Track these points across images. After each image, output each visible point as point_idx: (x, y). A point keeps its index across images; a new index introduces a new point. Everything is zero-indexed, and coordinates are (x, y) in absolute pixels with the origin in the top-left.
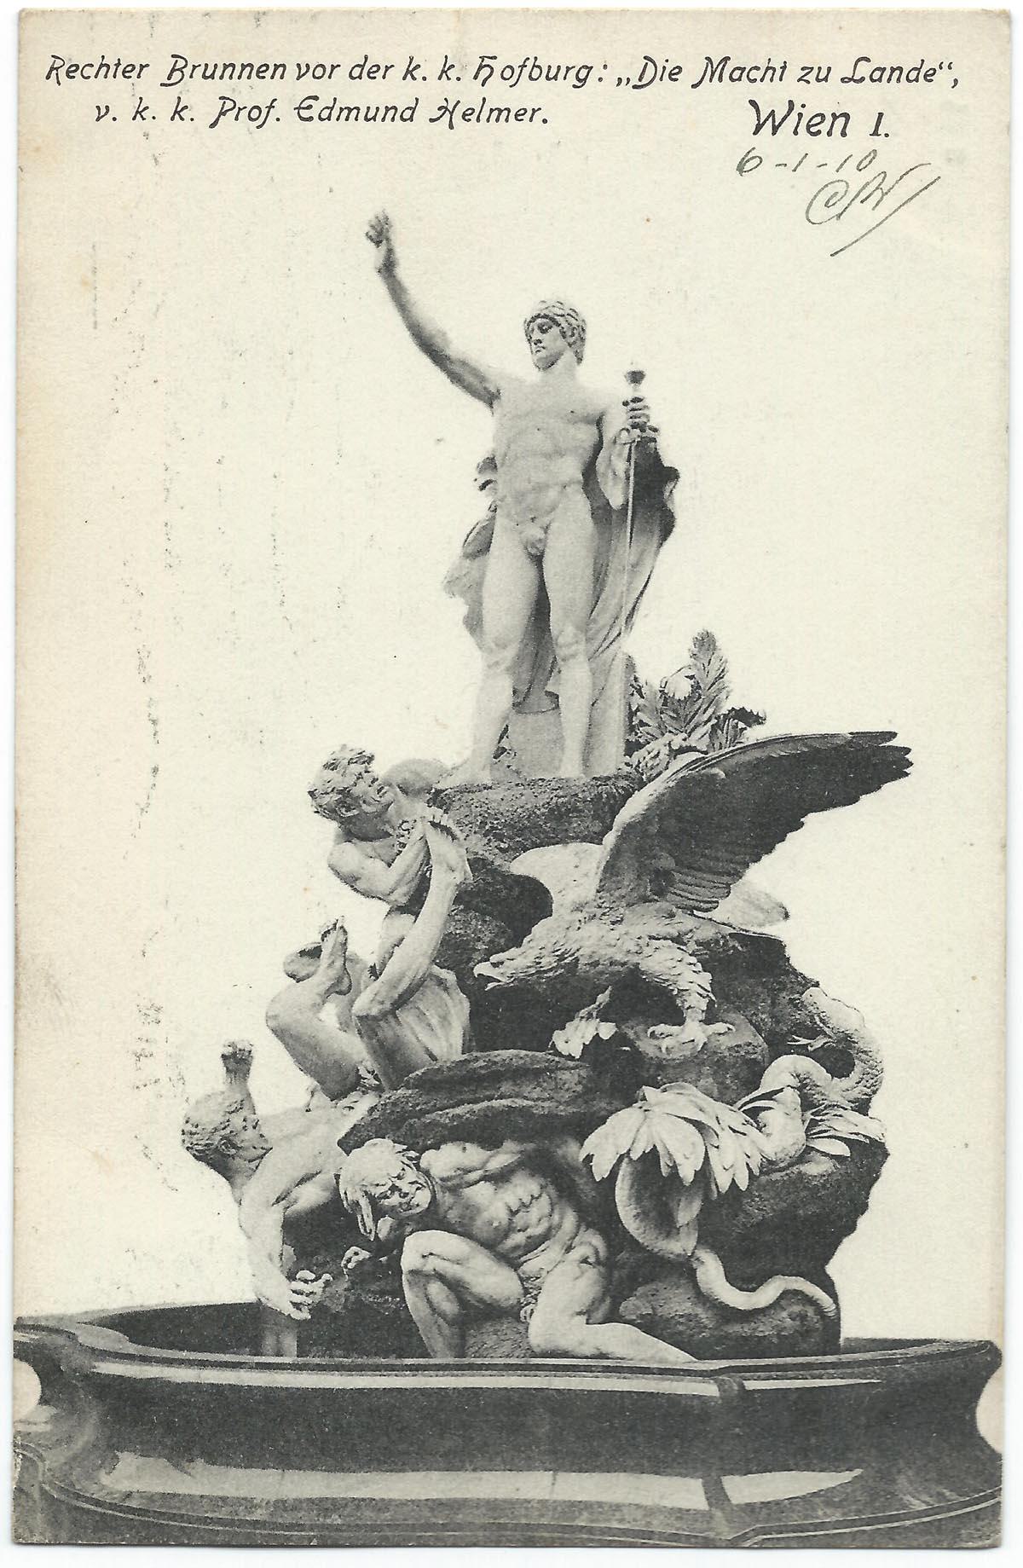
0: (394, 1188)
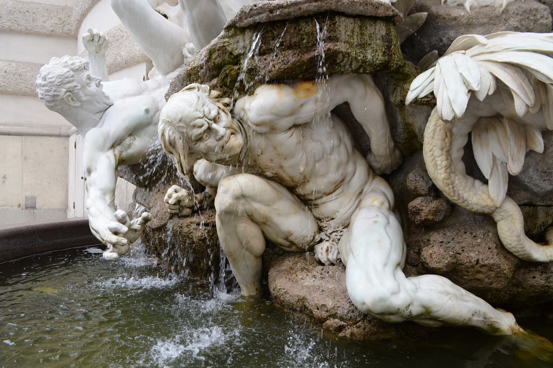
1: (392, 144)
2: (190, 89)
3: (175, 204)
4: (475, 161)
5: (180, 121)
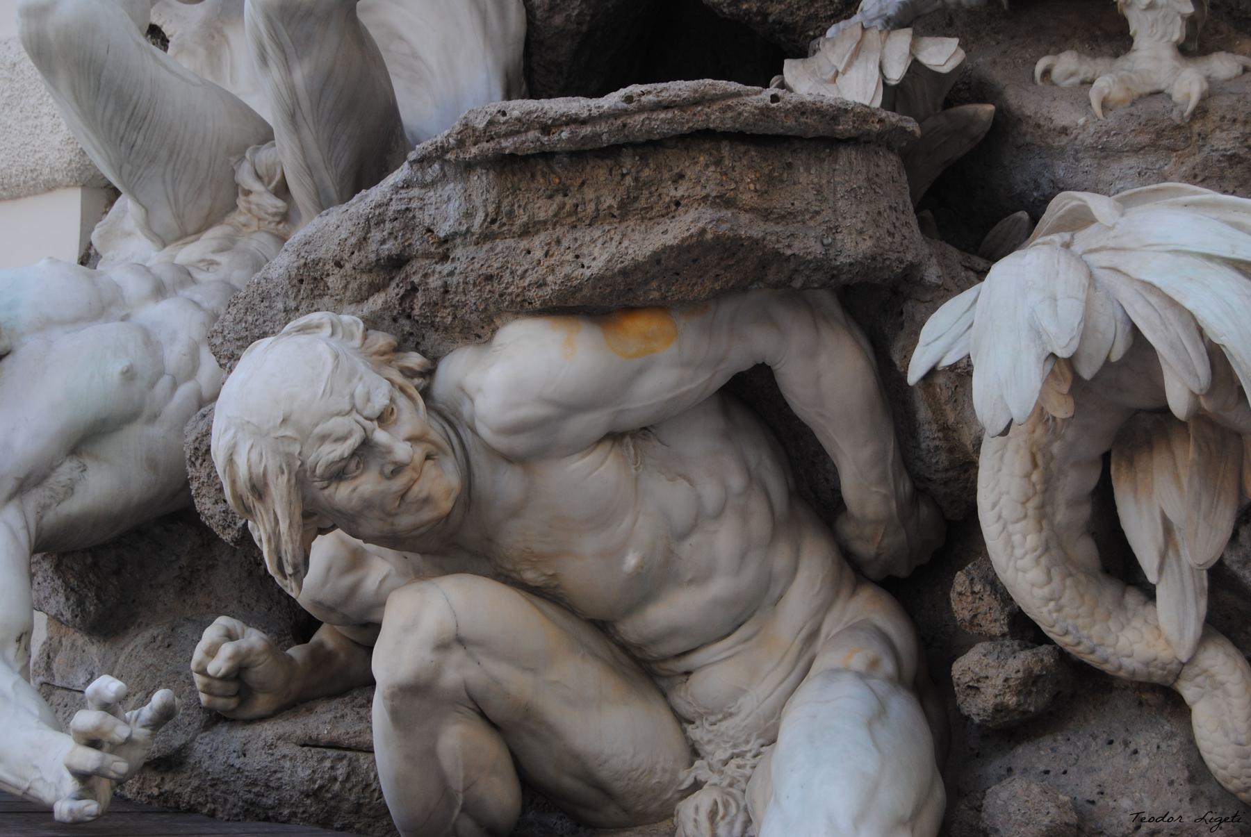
0: (366, 448)
1: (906, 487)
2: (303, 330)
3: (225, 678)
4: (1122, 532)
5: (285, 421)
